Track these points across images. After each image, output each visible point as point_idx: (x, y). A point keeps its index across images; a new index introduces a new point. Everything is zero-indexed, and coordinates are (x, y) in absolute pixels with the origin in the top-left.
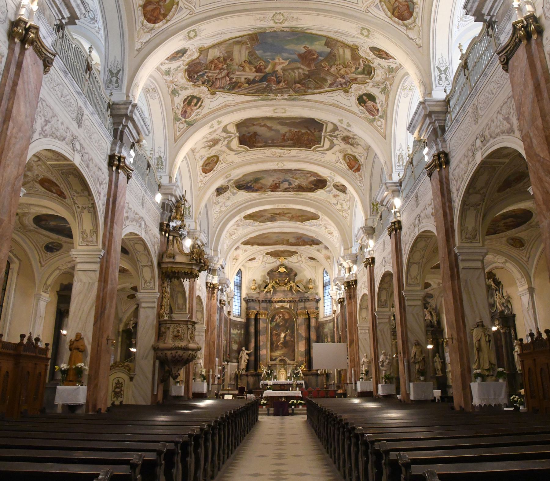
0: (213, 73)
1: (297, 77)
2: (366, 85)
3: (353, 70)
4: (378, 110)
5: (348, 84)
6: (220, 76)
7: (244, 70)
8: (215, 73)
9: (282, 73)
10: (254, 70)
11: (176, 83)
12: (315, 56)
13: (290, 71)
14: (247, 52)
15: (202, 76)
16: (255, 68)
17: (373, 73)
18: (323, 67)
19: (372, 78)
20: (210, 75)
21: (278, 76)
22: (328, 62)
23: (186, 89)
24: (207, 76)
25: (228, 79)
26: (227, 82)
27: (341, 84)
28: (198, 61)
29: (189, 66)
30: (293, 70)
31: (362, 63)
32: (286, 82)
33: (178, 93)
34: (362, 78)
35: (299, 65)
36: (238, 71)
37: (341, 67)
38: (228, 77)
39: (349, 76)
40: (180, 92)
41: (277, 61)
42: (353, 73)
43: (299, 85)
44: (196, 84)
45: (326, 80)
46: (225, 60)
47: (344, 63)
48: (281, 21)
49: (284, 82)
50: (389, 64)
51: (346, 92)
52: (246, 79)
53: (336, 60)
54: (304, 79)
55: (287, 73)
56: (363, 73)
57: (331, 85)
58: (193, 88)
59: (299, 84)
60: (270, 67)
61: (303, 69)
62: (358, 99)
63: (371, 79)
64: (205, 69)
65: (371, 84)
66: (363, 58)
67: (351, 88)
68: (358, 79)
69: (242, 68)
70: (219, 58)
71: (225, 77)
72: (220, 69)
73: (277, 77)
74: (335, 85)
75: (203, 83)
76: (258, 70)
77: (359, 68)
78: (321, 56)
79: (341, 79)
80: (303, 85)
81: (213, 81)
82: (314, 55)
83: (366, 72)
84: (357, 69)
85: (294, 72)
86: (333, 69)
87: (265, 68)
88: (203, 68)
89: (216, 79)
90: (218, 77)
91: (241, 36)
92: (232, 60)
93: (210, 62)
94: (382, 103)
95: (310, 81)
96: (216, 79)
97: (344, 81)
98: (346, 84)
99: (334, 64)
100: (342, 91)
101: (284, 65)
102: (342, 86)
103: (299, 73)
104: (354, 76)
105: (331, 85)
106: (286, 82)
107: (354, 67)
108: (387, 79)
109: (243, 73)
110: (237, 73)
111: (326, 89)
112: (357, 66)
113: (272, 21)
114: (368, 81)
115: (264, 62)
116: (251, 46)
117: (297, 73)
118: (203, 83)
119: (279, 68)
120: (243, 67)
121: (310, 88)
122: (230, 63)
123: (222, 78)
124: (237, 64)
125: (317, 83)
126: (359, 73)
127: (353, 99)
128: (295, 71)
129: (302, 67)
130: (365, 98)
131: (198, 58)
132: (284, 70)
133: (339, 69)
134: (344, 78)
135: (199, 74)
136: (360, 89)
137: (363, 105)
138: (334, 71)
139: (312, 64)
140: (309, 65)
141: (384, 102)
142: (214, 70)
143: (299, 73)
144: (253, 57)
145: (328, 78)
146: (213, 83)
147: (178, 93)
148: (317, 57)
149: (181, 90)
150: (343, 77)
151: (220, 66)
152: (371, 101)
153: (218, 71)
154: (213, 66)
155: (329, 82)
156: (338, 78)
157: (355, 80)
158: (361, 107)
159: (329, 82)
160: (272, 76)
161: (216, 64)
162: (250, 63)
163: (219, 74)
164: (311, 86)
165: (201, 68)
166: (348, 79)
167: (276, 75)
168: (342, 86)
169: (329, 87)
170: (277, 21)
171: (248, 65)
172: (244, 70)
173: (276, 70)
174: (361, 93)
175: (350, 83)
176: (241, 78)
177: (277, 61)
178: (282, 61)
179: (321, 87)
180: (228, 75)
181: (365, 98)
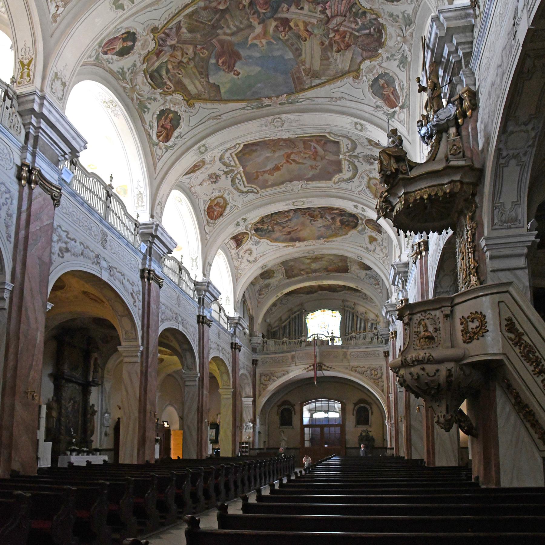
0: (348, 27)
1: (229, 20)
2: (142, 58)
3: (170, 67)
4: (106, 53)
5: (161, 42)
6: (339, 19)
7: (306, 24)
8: (345, 26)
9: (251, 20)
10: (292, 24)
11: (401, 34)
12: (220, 61)
13: (242, 26)
14: (303, 56)
15: (364, 27)
16: (290, 28)
17: (149, 80)
18: (203, 48)
19: (144, 73)
20: (353, 26)
21: (256, 16)
22: (202, 59)
23: (391, 15)
24: (357, 23)
25: (328, 12)
26: (330, 7)
27: (168, 35)
28: (365, 54)
29: (377, 50)
30: (240, 30)
31: (169, 83)
32: (241, 6)
33: (404, 16)
34: (153, 64)
35: (234, 39)
36: (313, 24)
37: (185, 60)
38: (327, 16)
39: (168, 54)
40: (401, 16)
41: (264, 41)
42: (166, 62)
43: (221, 7)
44: (374, 16)
45: (190, 31)
46: (331, 45)
47: (185, 68)
48: (275, 120)
49: (244, 6)
50: (151, 112)
51: (154, 30)
52: (302, 8)
53: (195, 66)
54: (218, 20)
55: (245, 22)
56: (158, 70)
57: (179, 27)
58: (382, 11)
59: (222, 10)
60: (271, 30)
61: (228, 35)
62: (134, 34)
63: (144, 71)
64: (358, 37)
65: (138, 64)
66: (173, 92)
67: (154, 39)
68: (155, 58)
69: (309, 28)
70: (338, 51)
71: (333, 17)
72: (337, 31)
73: (256, 12)
74: (174, 30)
75: (364, 13)
76: (285, 22)
77: (167, 73)
78: (214, 64)
79: (173, 42)
80: (216, 11)
81: (350, 13)
82: (223, 63)
83: (156, 74)
84: (168, 71)
85: (235, 26)
86: (190, 50)
87: (277, 27)
88: (360, 39)
89: (345, 16)
90: (344, 18)
91: (312, 87)
92: (322, 43)
93: (351, 45)
94: (110, 63)
95: (210, 21)
96: (345, 16)
97: (168, 43)
98: (162, 40)
99: (193, 59)
100: (160, 27)
101: (252, 36)
102: (164, 33)
103: (228, 27)
104: (164, 58)
105: (179, 27)
106: (241, 6)
107: (172, 71)
108: (133, 88)
109: (306, 19)
110: (314, 21)
111: (180, 18)
112: (169, 75)
113: (283, 119)
114: (145, 66)
115: (280, 38)
116: (299, 67)
117: (232, 27)
118: (364, 13)
119: (259, 29)
120: (307, 31)
121: (205, 8)
122: (324, 38)
123: (337, 15)
124: (316, 36)
125: (197, 21)
126: (160, 67)
127: (139, 29)
128: (235, 29)
129: (229, 38)
130: (130, 44)
131: (364, 59)
132: (250, 27)
133: (185, 56)
134: (171, 46)
135: (367, 32)
136: (143, 46)
137: (124, 36)
138: (188, 49)
139: (218, 48)
140: (222, 43)
141: (110, 65)
142: (345, 32)
143: (228, 27)
144: (295, 46)
145: (189, 35)
146: (350, 9)
147: (404, 16)
148: (217, 61)
149: (398, 16)
150: (173, 47)
151: (337, 37)
152: (121, 49)
153: (342, 29)
154: (347, 39)
155: (184, 30)
156: (178, 42)
157: (158, 54)
158: (123, 31)
159: (184, 30)
160: (264, 14)
161: (343, 41)
162: (299, 37)
163: (341, 24)
164: (203, 13)
165: (362, 41)
166: (166, 49)
167: (259, 17)
168: (164, 33)
169: (180, 22)
170: (279, 120)
171: (301, 33)
172: (306, 24)
173: (261, 26)
174: (138, 44)
175: (160, 45)
176: (310, 11)
177: (264, 41)
178: (256, 42)
179: (190, 16)
180: (329, 20)
181: (130, 44)
